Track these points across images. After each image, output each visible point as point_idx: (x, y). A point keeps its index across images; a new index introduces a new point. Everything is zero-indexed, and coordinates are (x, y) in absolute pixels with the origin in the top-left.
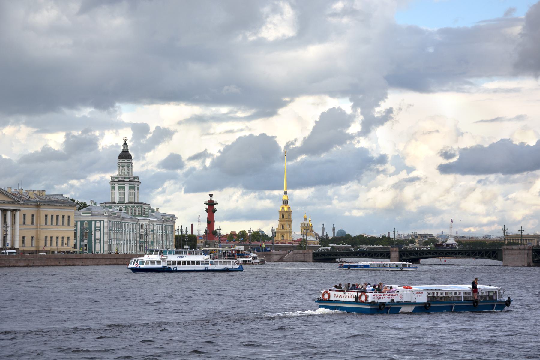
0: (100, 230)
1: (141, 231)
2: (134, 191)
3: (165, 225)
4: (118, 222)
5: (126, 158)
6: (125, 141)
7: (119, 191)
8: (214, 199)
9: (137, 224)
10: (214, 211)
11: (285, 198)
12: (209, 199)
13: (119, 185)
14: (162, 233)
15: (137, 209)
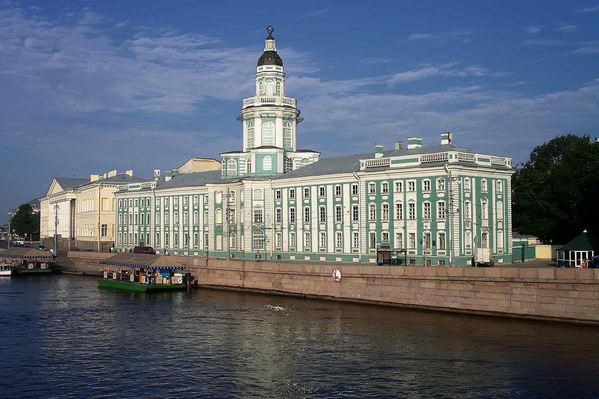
4: (145, 198)
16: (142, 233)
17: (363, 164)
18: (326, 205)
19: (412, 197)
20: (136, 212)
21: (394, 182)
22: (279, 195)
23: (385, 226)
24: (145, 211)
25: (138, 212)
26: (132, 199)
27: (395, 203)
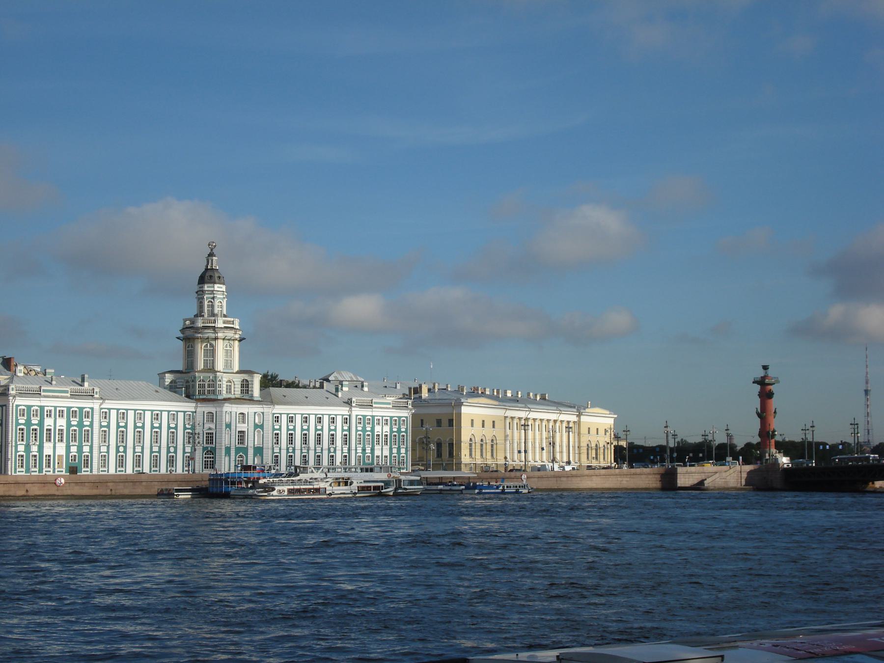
1: (207, 426)
4: (81, 409)
6: (212, 250)
9: (195, 412)
10: (770, 395)
12: (761, 373)
14: (349, 430)
16: (75, 454)
17: (354, 401)
18: (322, 431)
19: (387, 429)
21: (376, 418)
22: (277, 419)
23: (368, 450)
24: (81, 424)
25: (65, 425)
26: (53, 408)
27: (376, 434)
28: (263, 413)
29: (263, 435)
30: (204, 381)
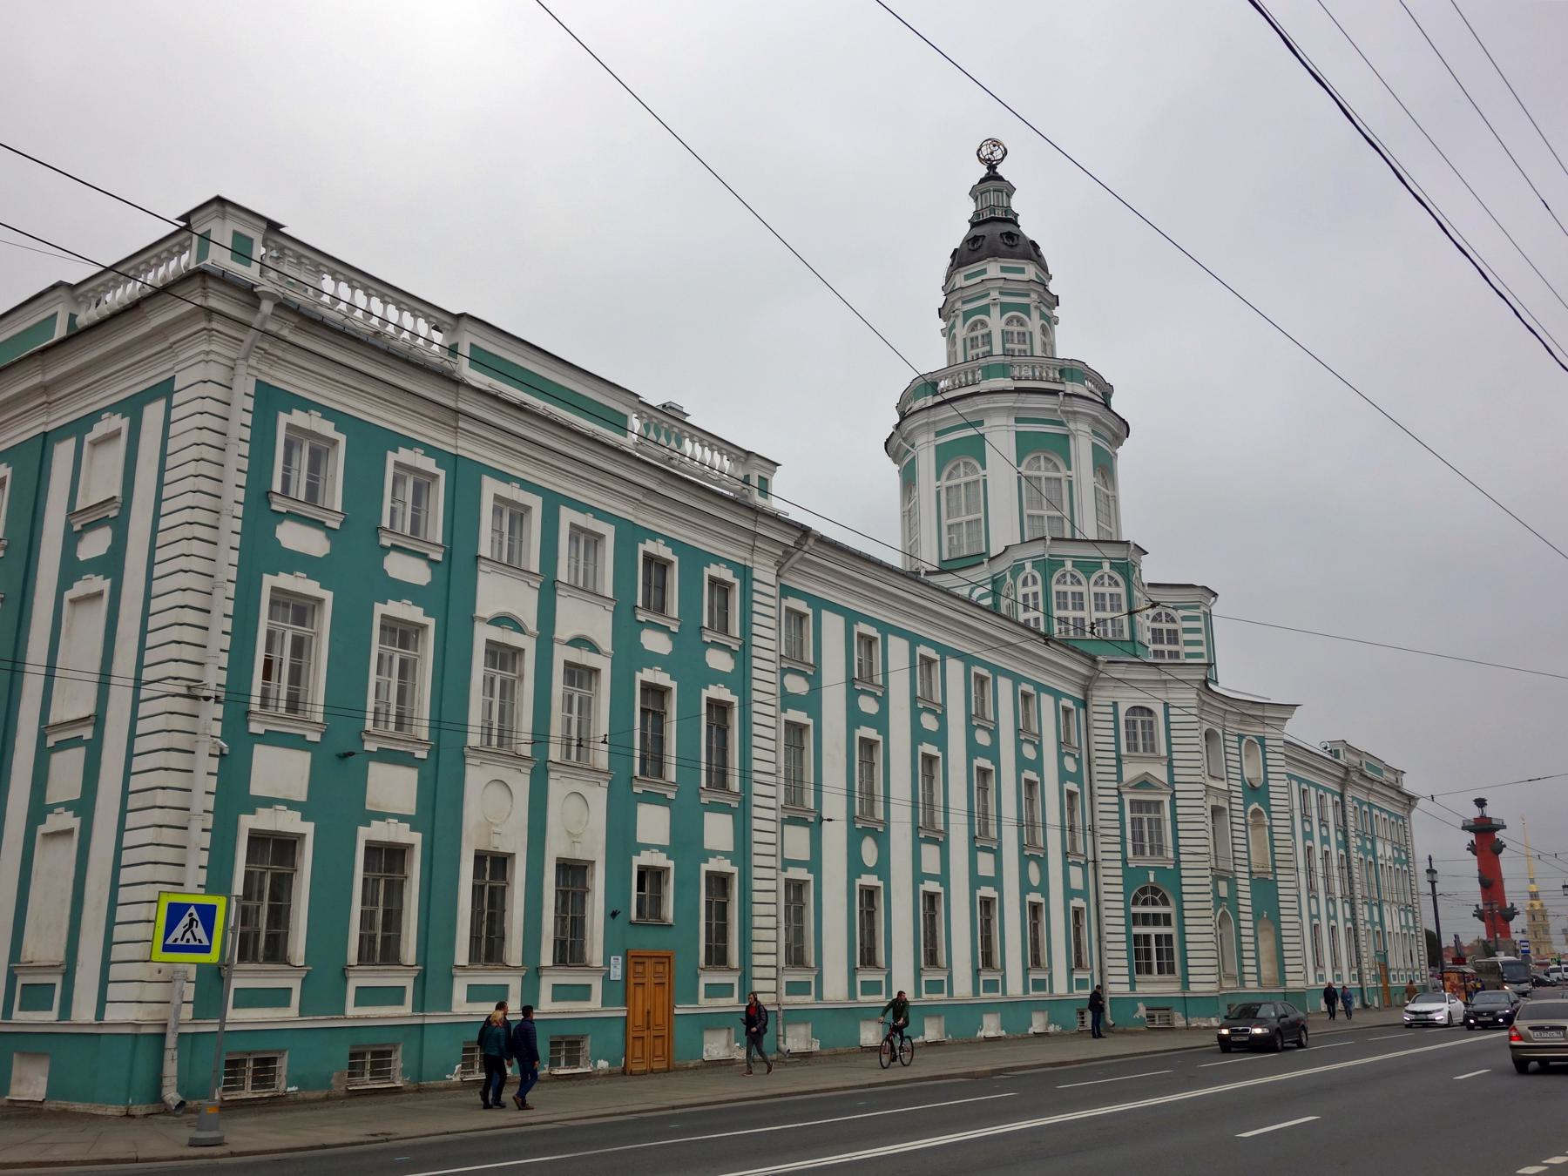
0: (112, 564)
2: (1063, 473)
3: (1361, 803)
4: (694, 558)
5: (995, 254)
6: (992, 167)
7: (945, 483)
8: (1490, 811)
9: (1084, 704)
10: (1498, 848)
11: (1534, 888)
12: (1475, 813)
13: (938, 434)
14: (1345, 844)
15: (1088, 589)
16: (659, 860)
20: (579, 642)
25: (605, 641)
28: (1262, 740)
29: (1270, 827)
30: (1079, 583)
